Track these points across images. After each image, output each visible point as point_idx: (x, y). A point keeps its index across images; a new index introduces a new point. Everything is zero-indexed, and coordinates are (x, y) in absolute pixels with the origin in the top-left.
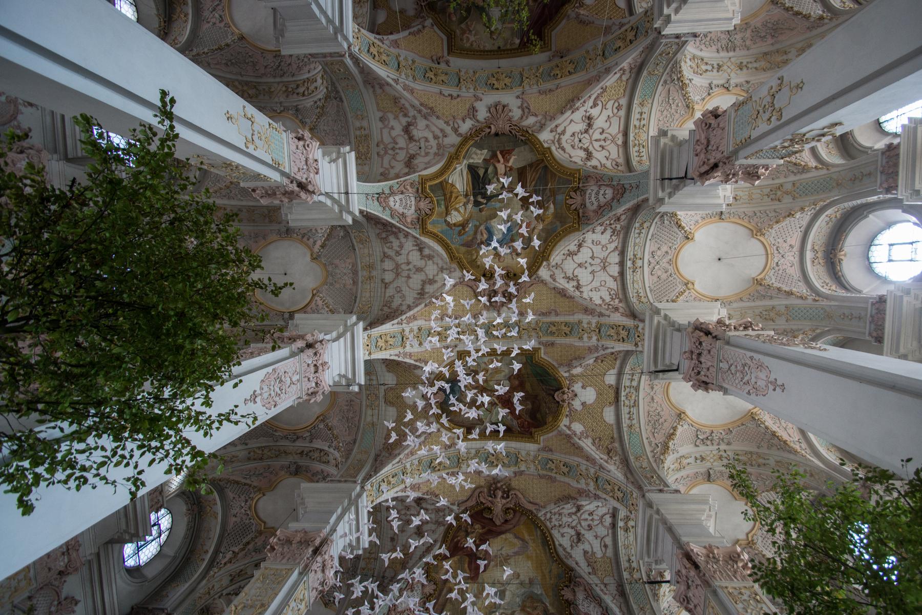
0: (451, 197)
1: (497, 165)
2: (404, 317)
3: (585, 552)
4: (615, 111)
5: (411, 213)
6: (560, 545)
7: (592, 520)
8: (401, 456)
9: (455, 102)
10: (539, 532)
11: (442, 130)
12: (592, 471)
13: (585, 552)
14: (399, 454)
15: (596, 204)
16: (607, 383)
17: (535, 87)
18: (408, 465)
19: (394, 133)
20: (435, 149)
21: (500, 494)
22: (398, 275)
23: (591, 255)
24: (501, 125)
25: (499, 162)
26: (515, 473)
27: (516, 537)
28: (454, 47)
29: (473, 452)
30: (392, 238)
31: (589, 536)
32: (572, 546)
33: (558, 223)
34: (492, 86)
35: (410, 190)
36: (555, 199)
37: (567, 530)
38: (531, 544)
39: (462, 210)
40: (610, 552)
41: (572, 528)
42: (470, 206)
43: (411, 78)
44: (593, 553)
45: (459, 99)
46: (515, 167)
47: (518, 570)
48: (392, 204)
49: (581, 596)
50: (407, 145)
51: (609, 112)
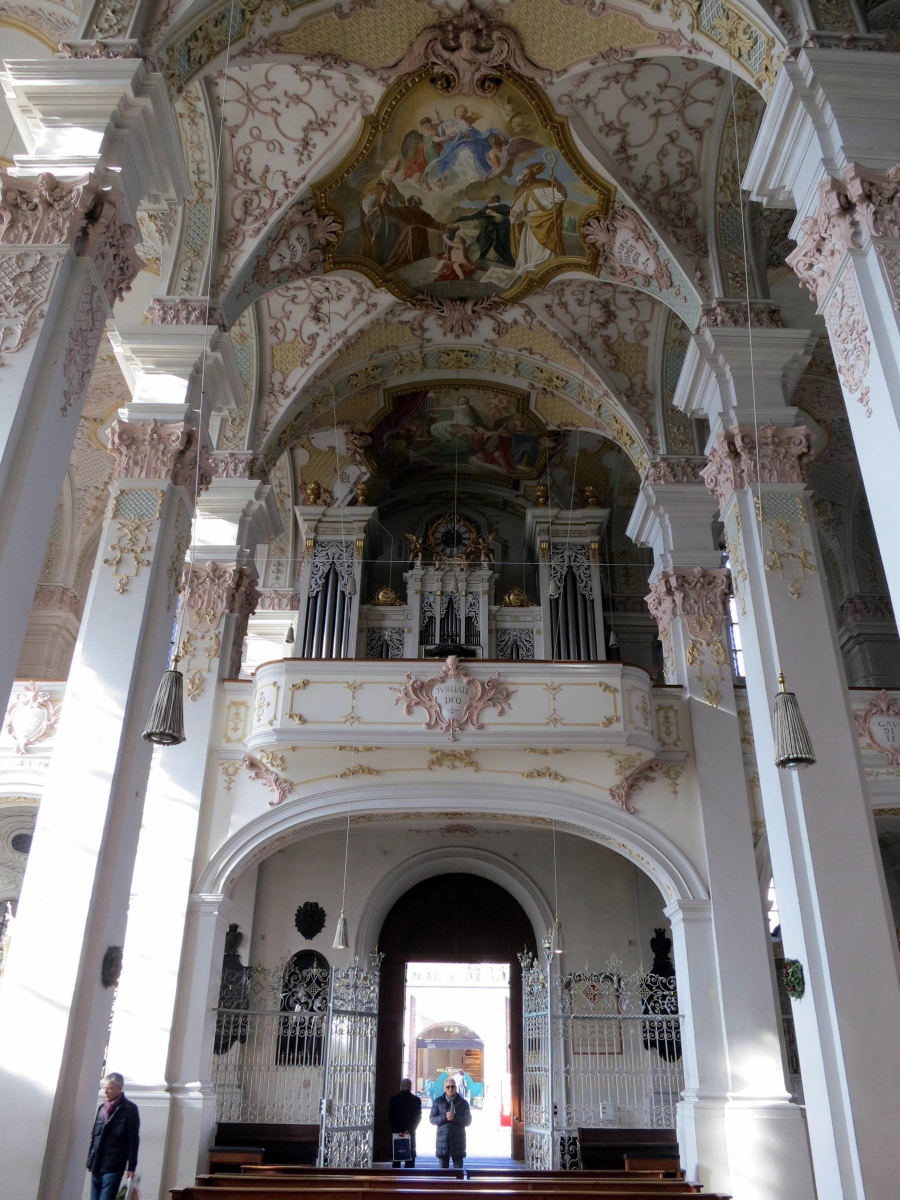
0: (549, 232)
1: (463, 261)
2: (684, 53)
4: (279, 326)
5: (624, 235)
9: (525, 345)
11: (552, 315)
15: (293, 241)
17: (404, 354)
19: (632, 313)
20: (568, 291)
22: (685, 93)
23: (281, 120)
24: (454, 314)
25: (461, 266)
28: (522, 400)
30: (675, 174)
33: (353, 185)
34: (468, 354)
35: (617, 266)
36: (363, 223)
39: (532, 205)
42: (517, 208)
43: (586, 389)
45: (520, 346)
46: (433, 259)
48: (652, 264)
50: (614, 296)
51: (289, 325)
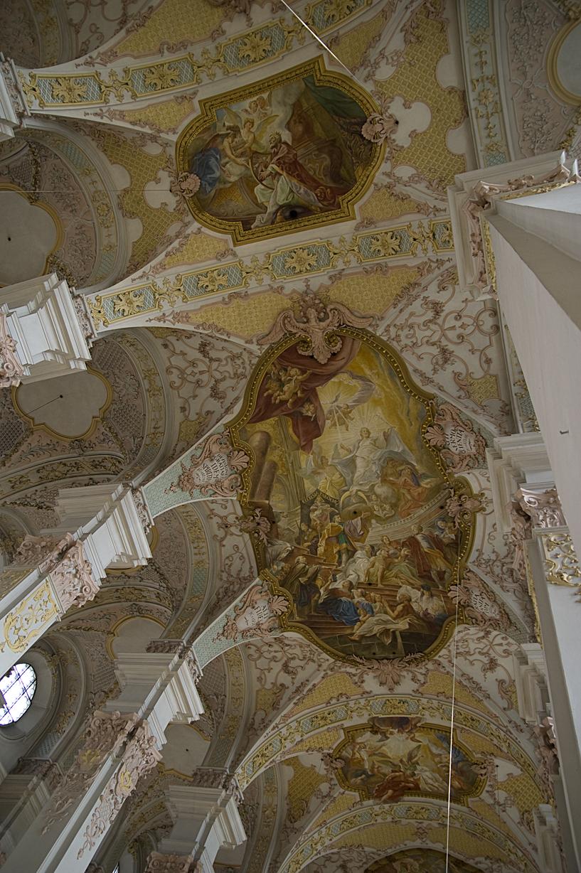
2: (94, 54)
3: (456, 375)
6: (416, 371)
7: (463, 326)
13: (456, 375)
16: (444, 86)
21: (312, 313)
29: (262, 259)
31: (461, 351)
32: (435, 371)
37: (426, 349)
38: (375, 380)
40: (495, 368)
41: (433, 344)
44: (469, 374)
47: (366, 426)
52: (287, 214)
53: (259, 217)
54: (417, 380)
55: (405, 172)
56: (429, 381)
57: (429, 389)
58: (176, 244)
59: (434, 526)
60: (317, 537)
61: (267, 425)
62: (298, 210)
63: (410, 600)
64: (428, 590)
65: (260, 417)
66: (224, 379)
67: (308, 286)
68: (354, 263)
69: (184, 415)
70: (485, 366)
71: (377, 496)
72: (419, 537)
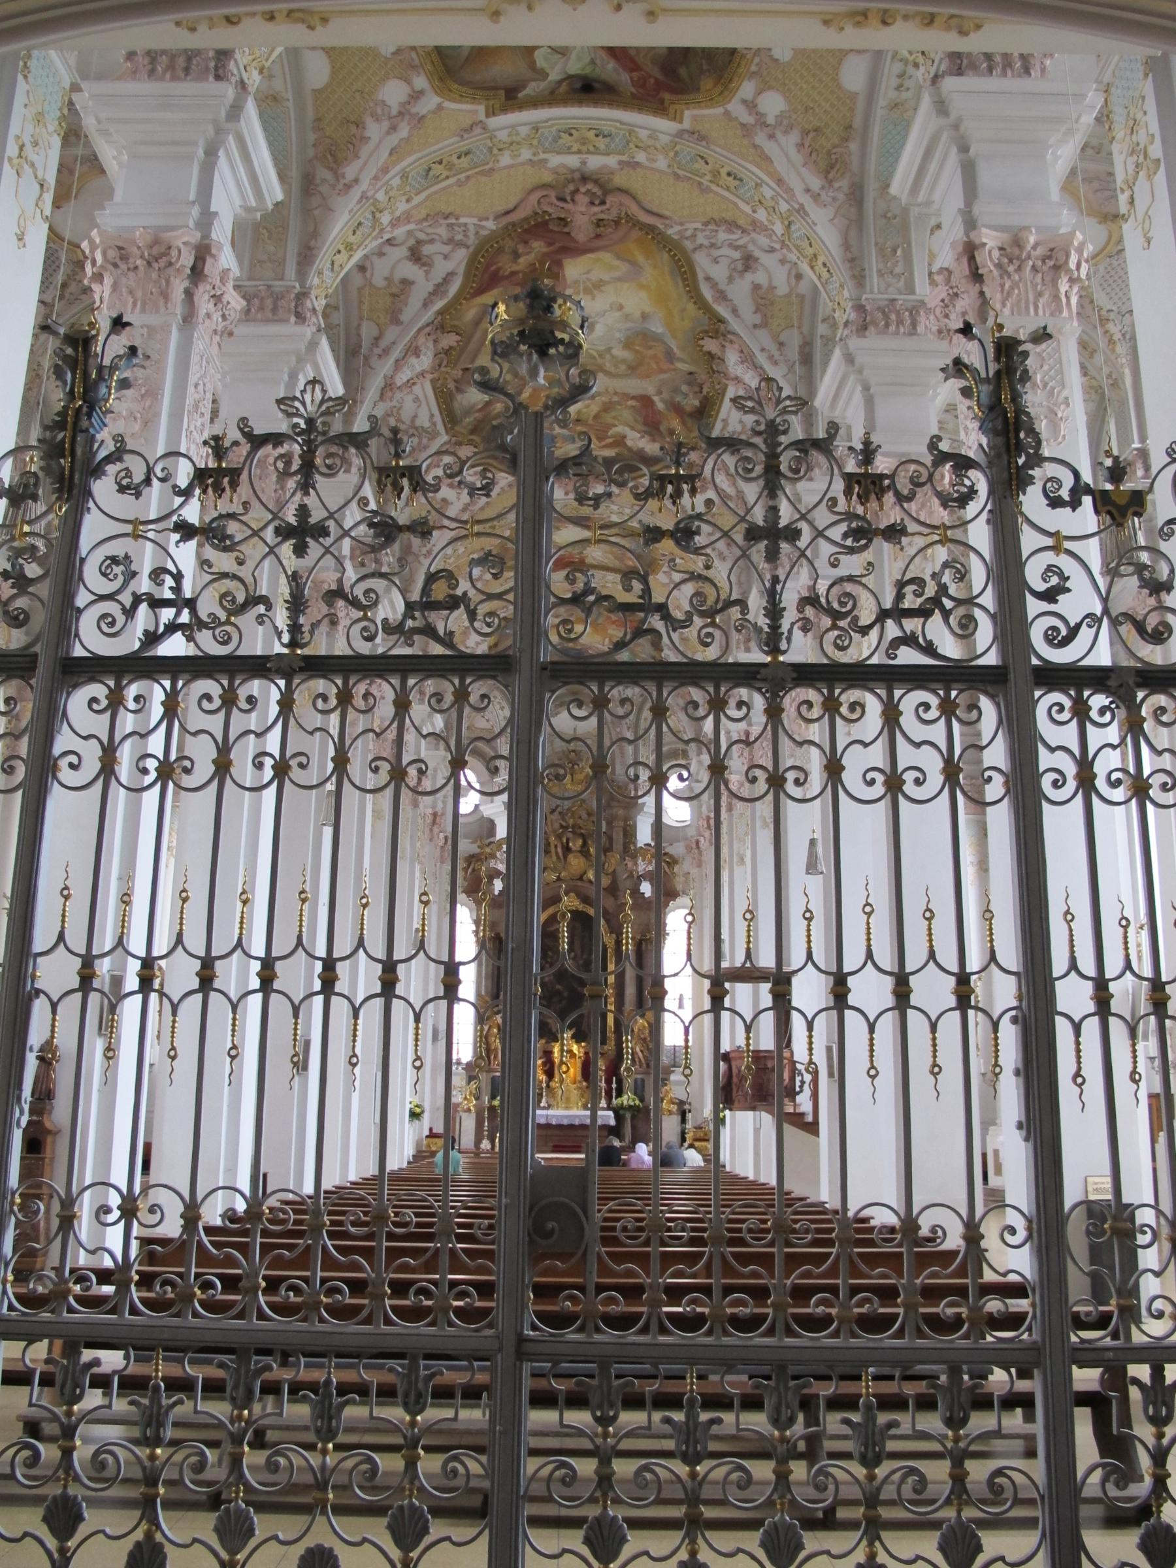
3: (756, 287)
6: (708, 279)
8: (364, 185)
10: (666, 256)
12: (784, 207)
14: (356, 181)
18: (381, 196)
26: (620, 163)
27: (618, 257)
29: (524, 131)
32: (731, 279)
41: (736, 248)
47: (621, 300)
49: (732, 358)
52: (578, 85)
53: (533, 85)
54: (707, 293)
55: (773, 104)
56: (722, 296)
57: (722, 310)
58: (404, 131)
59: (676, 390)
60: (524, 386)
61: (487, 298)
62: (597, 85)
63: (624, 437)
64: (651, 435)
65: (481, 291)
66: (431, 241)
67: (584, 163)
68: (662, 163)
69: (365, 278)
70: (793, 281)
71: (613, 357)
72: (655, 398)
